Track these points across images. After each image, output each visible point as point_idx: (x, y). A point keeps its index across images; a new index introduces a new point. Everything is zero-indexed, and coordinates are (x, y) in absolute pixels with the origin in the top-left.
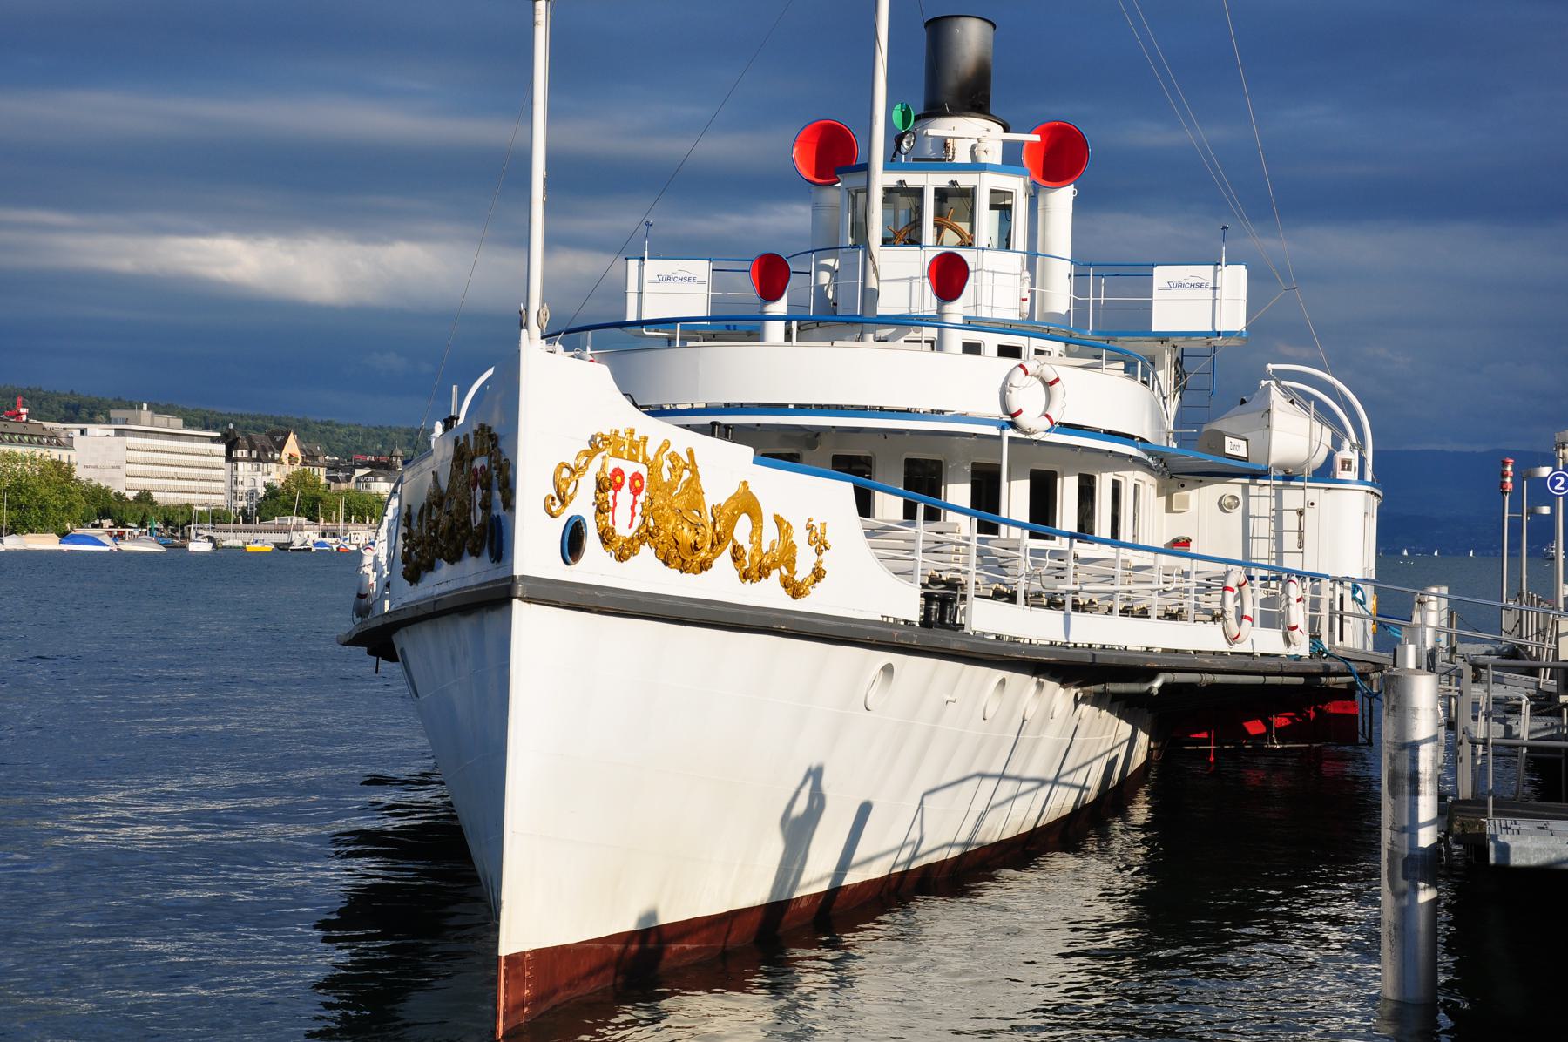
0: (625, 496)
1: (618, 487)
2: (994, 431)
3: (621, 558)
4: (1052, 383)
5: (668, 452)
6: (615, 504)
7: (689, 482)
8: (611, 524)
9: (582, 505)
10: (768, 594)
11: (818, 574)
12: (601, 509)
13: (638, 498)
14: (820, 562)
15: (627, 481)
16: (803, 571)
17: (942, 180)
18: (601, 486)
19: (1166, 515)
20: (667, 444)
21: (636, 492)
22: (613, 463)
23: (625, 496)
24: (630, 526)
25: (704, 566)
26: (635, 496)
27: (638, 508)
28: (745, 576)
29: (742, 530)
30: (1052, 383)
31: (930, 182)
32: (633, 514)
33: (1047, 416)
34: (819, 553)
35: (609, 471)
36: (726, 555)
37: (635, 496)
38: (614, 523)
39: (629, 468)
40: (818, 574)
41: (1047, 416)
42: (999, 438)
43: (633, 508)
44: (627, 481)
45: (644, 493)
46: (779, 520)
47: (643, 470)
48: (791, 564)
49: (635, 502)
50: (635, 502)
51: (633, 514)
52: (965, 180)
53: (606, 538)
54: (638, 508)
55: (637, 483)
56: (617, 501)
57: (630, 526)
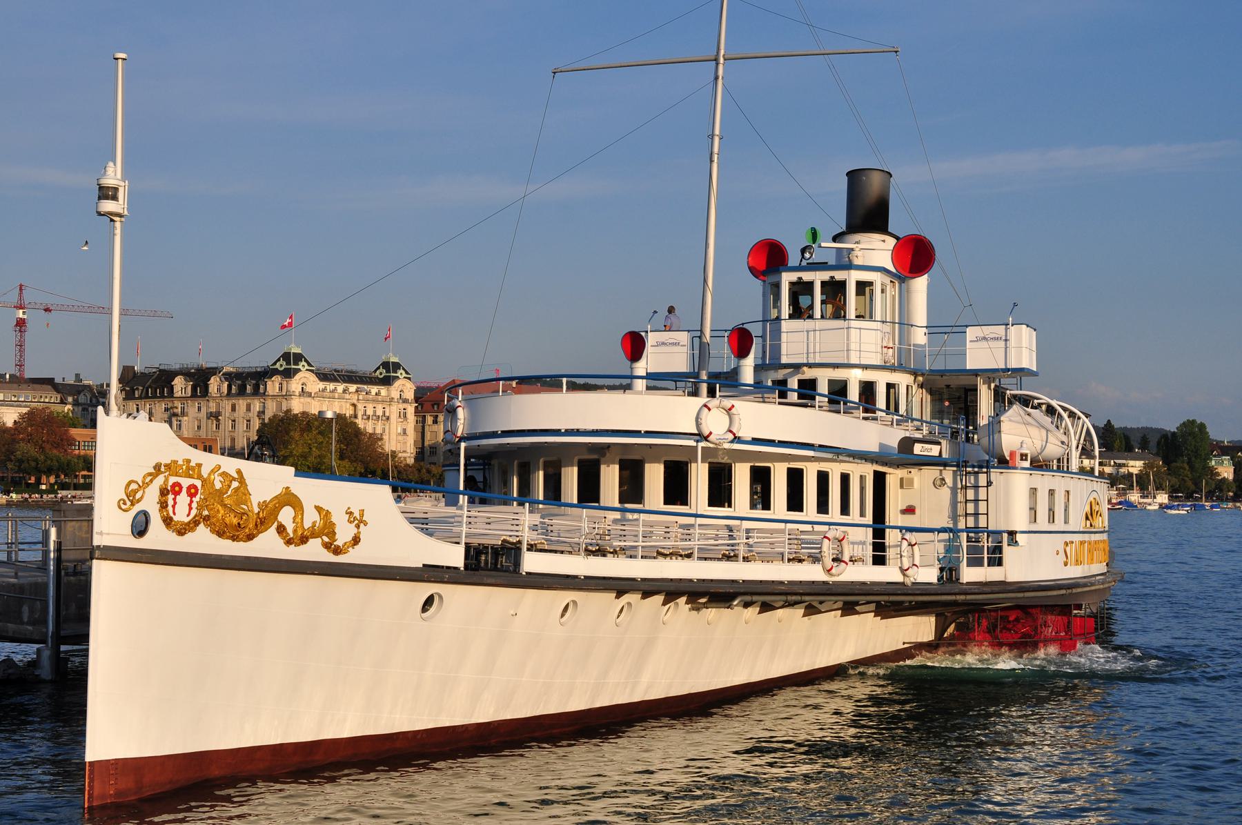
0: (183, 499)
1: (177, 493)
2: (692, 443)
4: (730, 409)
5: (220, 471)
6: (175, 503)
7: (237, 489)
8: (171, 514)
9: (150, 502)
10: (314, 551)
11: (356, 540)
12: (163, 505)
13: (194, 499)
14: (359, 533)
15: (184, 490)
18: (164, 492)
19: (900, 490)
21: (192, 495)
22: (172, 480)
23: (183, 499)
24: (188, 515)
25: (250, 537)
26: (191, 498)
27: (194, 505)
28: (289, 542)
29: (286, 516)
30: (730, 409)
32: (191, 509)
33: (731, 431)
34: (358, 527)
35: (170, 483)
36: (272, 530)
37: (191, 498)
38: (174, 514)
39: (186, 482)
40: (356, 540)
41: (731, 431)
42: (697, 446)
43: (190, 505)
44: (184, 490)
45: (198, 496)
46: (319, 509)
47: (198, 483)
48: (331, 532)
49: (191, 502)
50: (191, 502)
51: (191, 509)
53: (168, 521)
54: (194, 505)
55: (193, 491)
56: (177, 500)
57: (188, 515)
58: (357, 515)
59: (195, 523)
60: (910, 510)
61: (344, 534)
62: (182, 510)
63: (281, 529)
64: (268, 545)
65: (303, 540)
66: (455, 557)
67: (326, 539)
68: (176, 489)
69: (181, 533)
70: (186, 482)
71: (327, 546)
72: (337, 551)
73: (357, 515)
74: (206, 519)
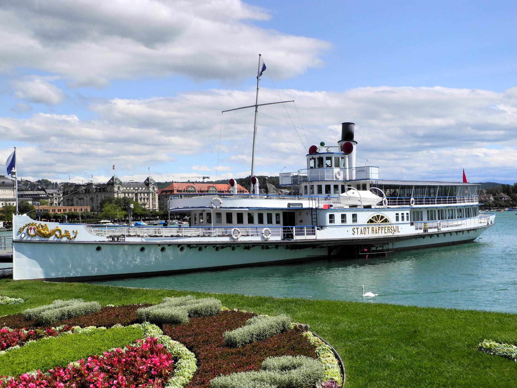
0: (32, 230)
3: (32, 237)
9: (25, 231)
10: (65, 239)
13: (36, 230)
16: (71, 237)
17: (318, 156)
18: (28, 230)
20: (40, 224)
22: (30, 227)
23: (32, 230)
31: (316, 156)
39: (33, 227)
40: (75, 237)
46: (66, 231)
47: (35, 227)
52: (322, 156)
53: (29, 235)
58: (75, 231)
59: (35, 235)
60: (301, 221)
61: (72, 236)
62: (32, 233)
63: (56, 235)
64: (51, 239)
65: (61, 237)
66: (104, 239)
67: (68, 237)
68: (31, 229)
69: (32, 236)
70: (33, 227)
71: (67, 238)
72: (70, 239)
73: (75, 231)
74: (37, 234)
